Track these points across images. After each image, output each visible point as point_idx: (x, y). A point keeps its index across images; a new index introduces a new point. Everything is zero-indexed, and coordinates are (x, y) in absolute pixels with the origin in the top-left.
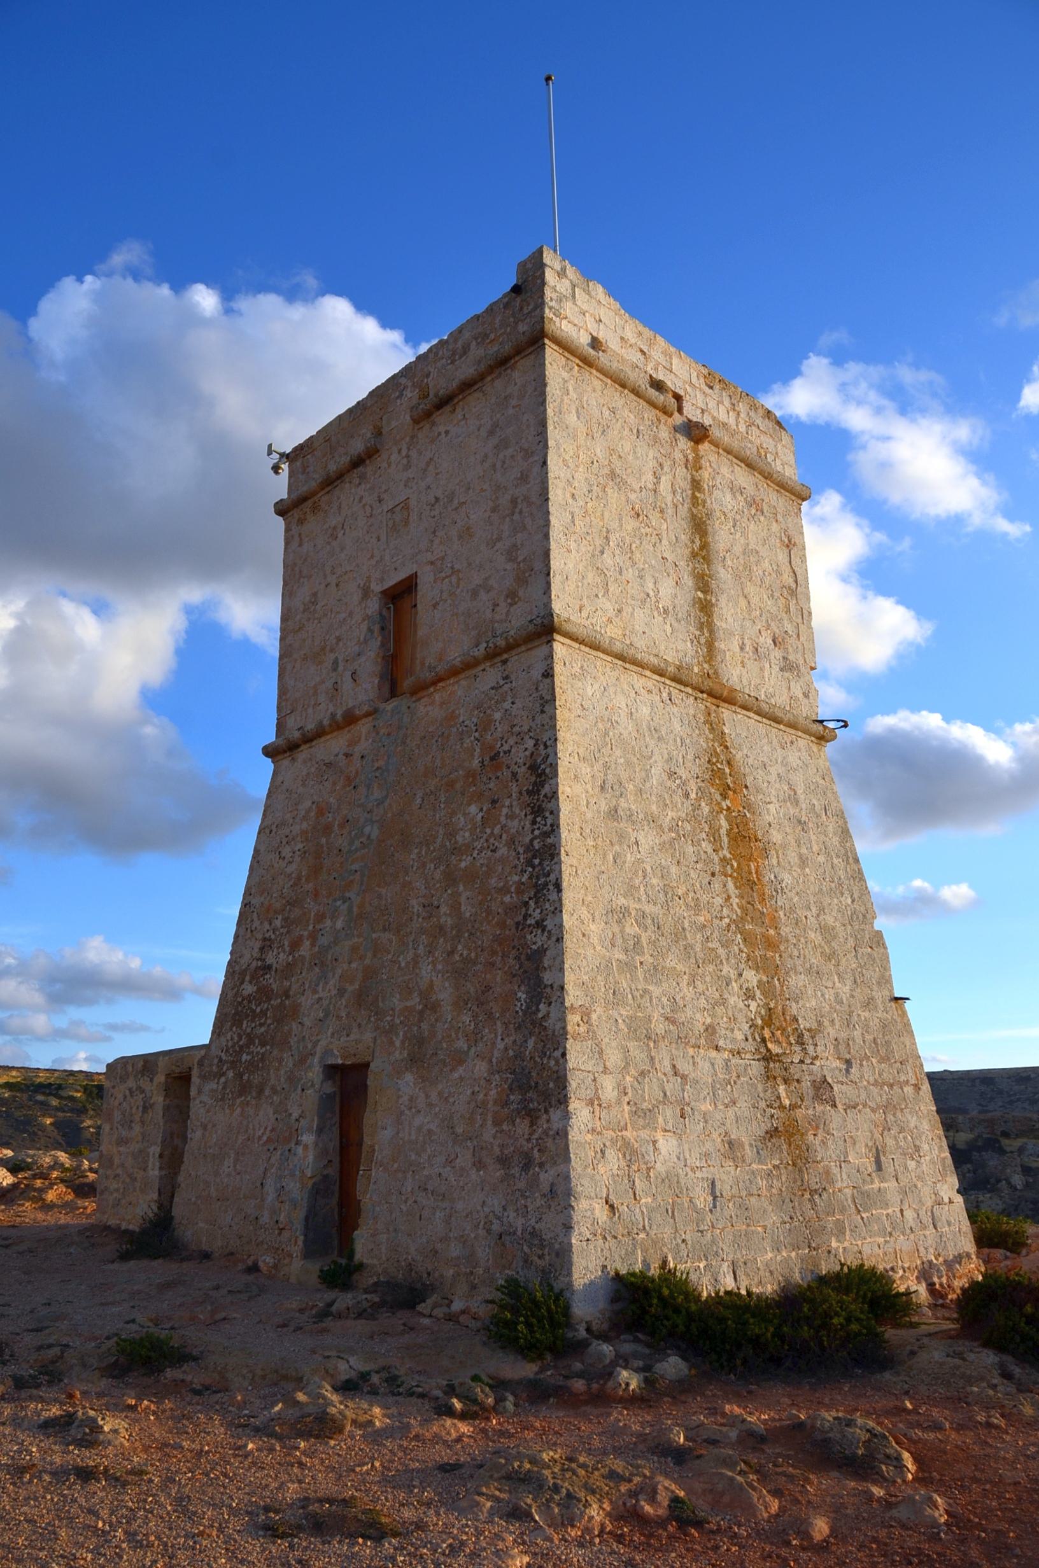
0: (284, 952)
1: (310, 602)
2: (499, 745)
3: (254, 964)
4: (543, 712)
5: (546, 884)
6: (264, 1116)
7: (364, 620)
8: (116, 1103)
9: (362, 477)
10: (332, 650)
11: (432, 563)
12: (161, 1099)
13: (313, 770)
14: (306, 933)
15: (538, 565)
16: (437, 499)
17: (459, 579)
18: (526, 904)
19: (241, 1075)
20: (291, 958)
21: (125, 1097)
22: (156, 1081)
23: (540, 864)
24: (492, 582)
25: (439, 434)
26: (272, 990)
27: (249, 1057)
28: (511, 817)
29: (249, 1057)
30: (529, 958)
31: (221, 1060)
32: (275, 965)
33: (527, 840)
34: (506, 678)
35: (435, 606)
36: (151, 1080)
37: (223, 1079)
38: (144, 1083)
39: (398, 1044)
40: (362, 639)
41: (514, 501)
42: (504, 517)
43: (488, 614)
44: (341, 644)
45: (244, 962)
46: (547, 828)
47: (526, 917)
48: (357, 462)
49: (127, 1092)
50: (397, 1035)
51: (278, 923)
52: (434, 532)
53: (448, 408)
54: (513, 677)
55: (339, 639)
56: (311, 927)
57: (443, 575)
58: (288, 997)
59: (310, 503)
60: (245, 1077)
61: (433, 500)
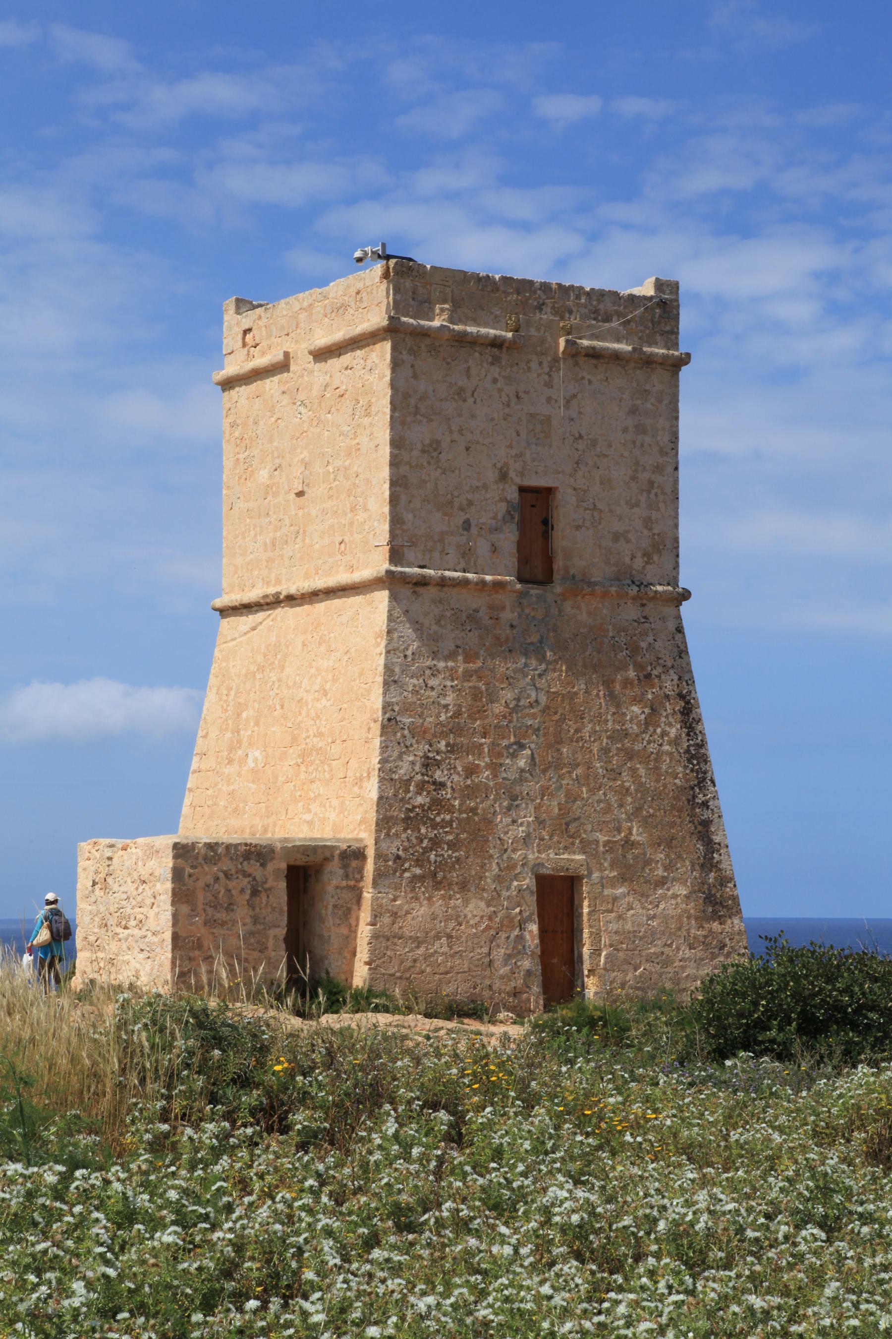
0: (458, 774)
1: (431, 445)
2: (649, 668)
3: (419, 777)
4: (680, 657)
5: (704, 779)
6: (475, 909)
7: (501, 500)
8: (201, 884)
9: (496, 361)
10: (462, 509)
11: (575, 489)
12: (283, 884)
13: (448, 614)
14: (483, 764)
15: (669, 545)
16: (581, 437)
17: (601, 518)
18: (692, 788)
19: (434, 875)
20: (469, 782)
21: (217, 879)
22: (270, 867)
23: (698, 764)
24: (630, 536)
25: (583, 378)
26: (454, 806)
27: (439, 859)
28: (670, 725)
29: (439, 859)
30: (700, 824)
31: (398, 857)
32: (449, 784)
33: (685, 745)
34: (645, 617)
35: (578, 527)
36: (263, 865)
37: (407, 875)
38: (253, 868)
39: (606, 864)
40: (500, 517)
41: (651, 483)
42: (643, 491)
43: (627, 560)
44: (473, 509)
45: (403, 771)
46: (699, 741)
47: (694, 797)
48: (496, 344)
49: (221, 875)
50: (605, 859)
51: (442, 745)
52: (577, 463)
53: (594, 361)
54: (651, 620)
55: (470, 503)
56: (487, 760)
57: (584, 504)
58: (477, 814)
59: (428, 341)
60: (440, 875)
61: (577, 435)
